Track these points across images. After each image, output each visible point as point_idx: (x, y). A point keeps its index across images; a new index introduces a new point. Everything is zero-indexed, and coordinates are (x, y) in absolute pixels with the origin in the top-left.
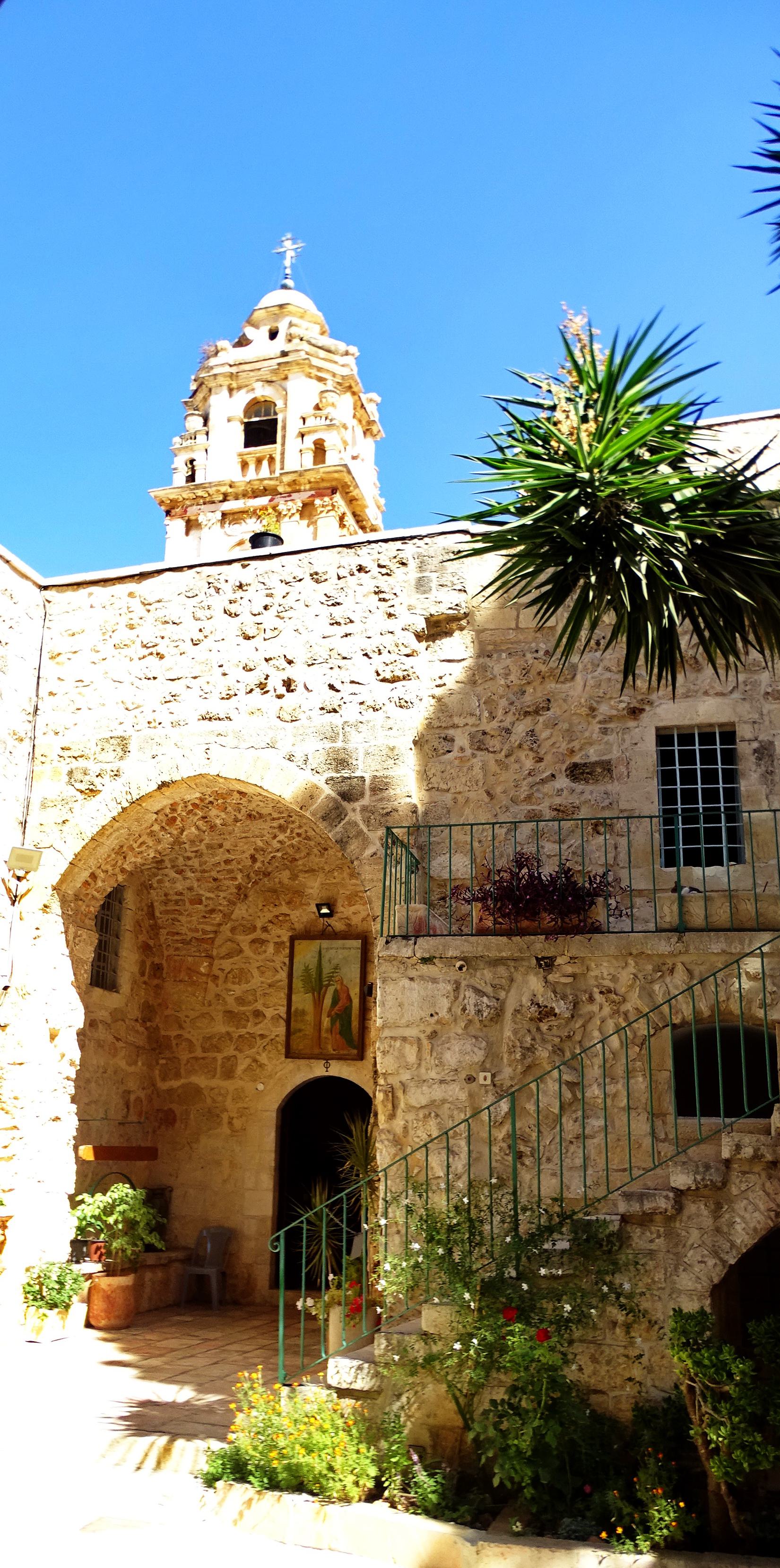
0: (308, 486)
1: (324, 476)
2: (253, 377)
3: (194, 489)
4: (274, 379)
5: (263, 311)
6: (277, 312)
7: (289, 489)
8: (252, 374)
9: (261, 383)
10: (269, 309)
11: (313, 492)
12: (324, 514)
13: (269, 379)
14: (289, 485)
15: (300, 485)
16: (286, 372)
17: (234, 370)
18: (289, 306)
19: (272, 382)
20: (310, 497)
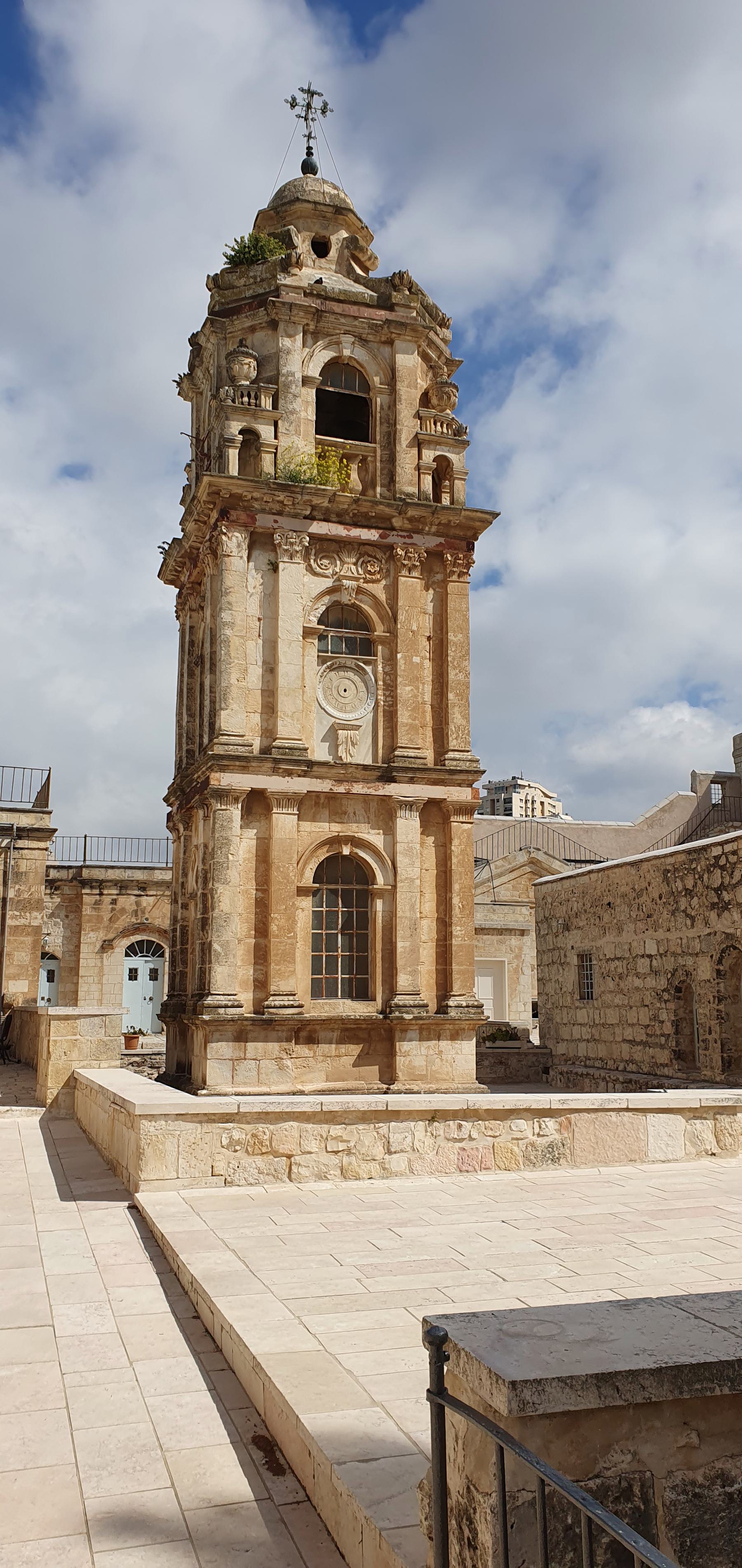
0: (434, 529)
1: (464, 521)
2: (344, 324)
3: (275, 490)
4: (371, 338)
5: (311, 206)
6: (328, 215)
7: (408, 526)
8: (343, 320)
9: (350, 339)
10: (319, 207)
11: (442, 540)
12: (455, 578)
13: (364, 336)
14: (411, 520)
15: (425, 524)
16: (393, 335)
17: (315, 303)
18: (351, 215)
19: (365, 341)
20: (437, 545)
